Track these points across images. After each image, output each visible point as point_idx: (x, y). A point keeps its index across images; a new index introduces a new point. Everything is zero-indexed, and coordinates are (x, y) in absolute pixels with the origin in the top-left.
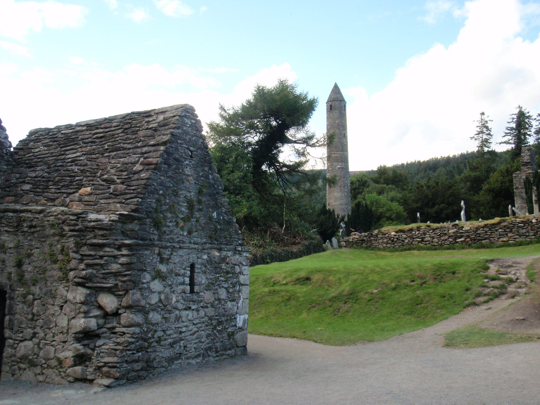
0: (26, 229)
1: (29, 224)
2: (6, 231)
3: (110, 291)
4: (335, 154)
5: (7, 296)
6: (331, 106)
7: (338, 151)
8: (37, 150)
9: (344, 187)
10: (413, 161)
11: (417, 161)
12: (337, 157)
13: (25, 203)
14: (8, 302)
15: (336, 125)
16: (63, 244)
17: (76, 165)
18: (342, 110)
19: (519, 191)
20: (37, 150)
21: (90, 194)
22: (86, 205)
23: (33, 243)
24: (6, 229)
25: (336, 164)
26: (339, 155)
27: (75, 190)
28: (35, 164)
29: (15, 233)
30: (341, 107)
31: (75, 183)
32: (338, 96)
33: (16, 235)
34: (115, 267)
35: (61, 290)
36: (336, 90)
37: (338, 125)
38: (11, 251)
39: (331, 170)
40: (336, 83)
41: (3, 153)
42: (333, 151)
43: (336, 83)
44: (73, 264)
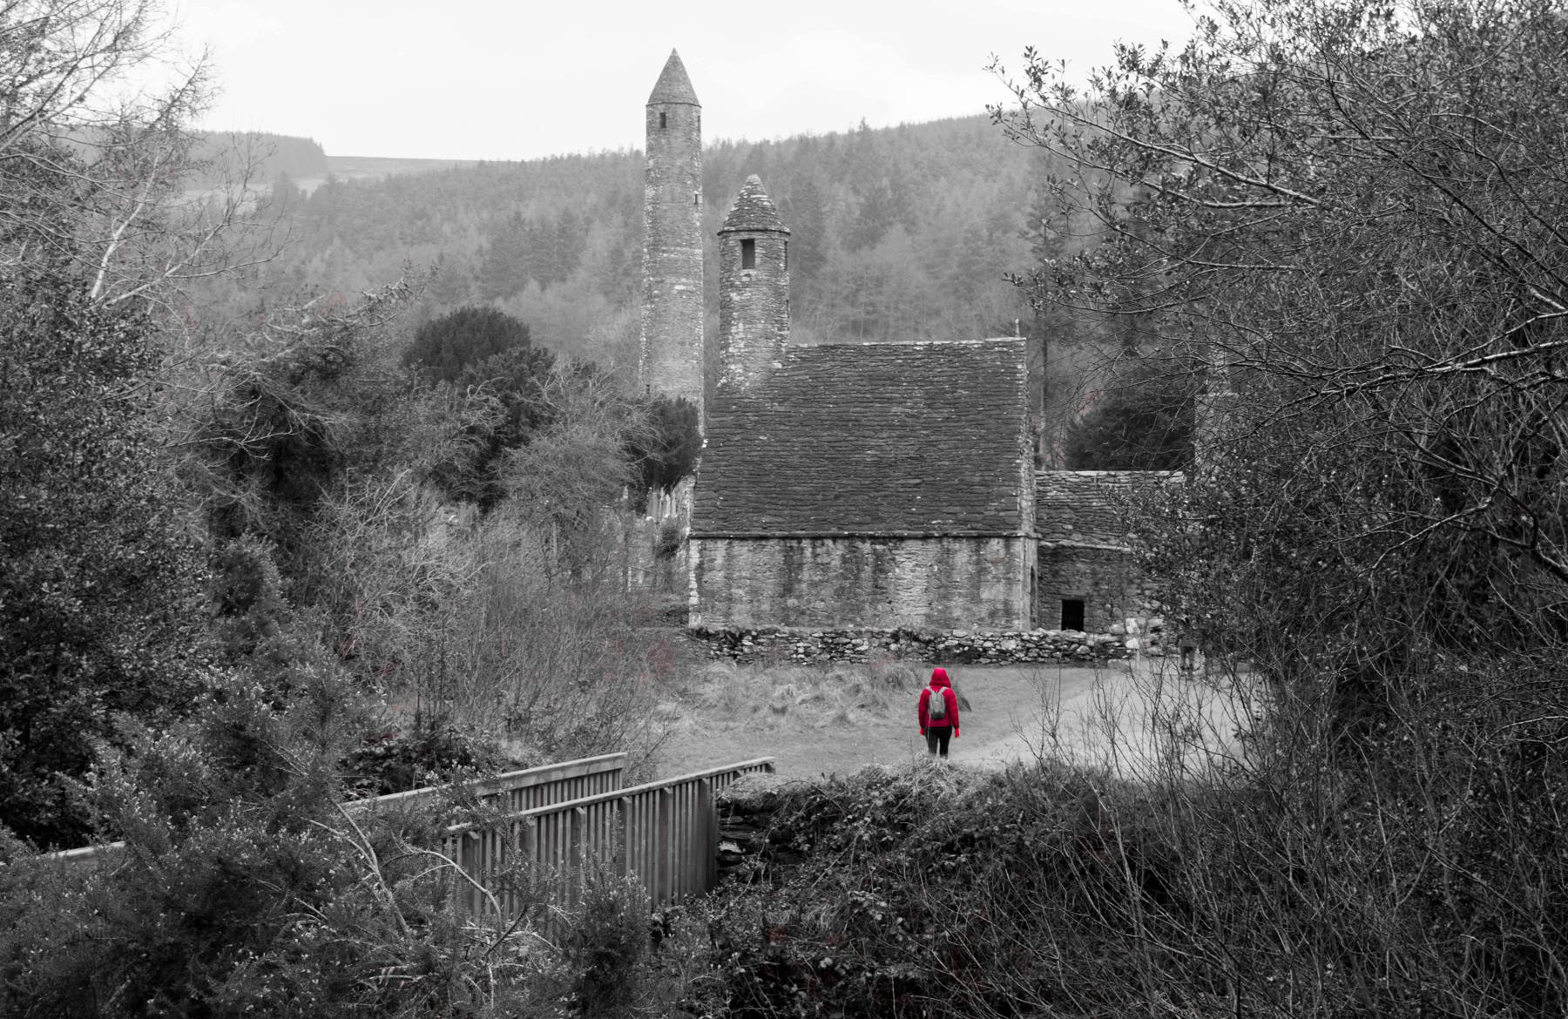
4: (672, 252)
6: (663, 115)
12: (676, 261)
14: (1086, 609)
15: (677, 171)
18: (691, 132)
25: (673, 280)
32: (682, 89)
36: (673, 70)
37: (681, 173)
39: (657, 296)
40: (674, 51)
42: (666, 244)
43: (674, 51)
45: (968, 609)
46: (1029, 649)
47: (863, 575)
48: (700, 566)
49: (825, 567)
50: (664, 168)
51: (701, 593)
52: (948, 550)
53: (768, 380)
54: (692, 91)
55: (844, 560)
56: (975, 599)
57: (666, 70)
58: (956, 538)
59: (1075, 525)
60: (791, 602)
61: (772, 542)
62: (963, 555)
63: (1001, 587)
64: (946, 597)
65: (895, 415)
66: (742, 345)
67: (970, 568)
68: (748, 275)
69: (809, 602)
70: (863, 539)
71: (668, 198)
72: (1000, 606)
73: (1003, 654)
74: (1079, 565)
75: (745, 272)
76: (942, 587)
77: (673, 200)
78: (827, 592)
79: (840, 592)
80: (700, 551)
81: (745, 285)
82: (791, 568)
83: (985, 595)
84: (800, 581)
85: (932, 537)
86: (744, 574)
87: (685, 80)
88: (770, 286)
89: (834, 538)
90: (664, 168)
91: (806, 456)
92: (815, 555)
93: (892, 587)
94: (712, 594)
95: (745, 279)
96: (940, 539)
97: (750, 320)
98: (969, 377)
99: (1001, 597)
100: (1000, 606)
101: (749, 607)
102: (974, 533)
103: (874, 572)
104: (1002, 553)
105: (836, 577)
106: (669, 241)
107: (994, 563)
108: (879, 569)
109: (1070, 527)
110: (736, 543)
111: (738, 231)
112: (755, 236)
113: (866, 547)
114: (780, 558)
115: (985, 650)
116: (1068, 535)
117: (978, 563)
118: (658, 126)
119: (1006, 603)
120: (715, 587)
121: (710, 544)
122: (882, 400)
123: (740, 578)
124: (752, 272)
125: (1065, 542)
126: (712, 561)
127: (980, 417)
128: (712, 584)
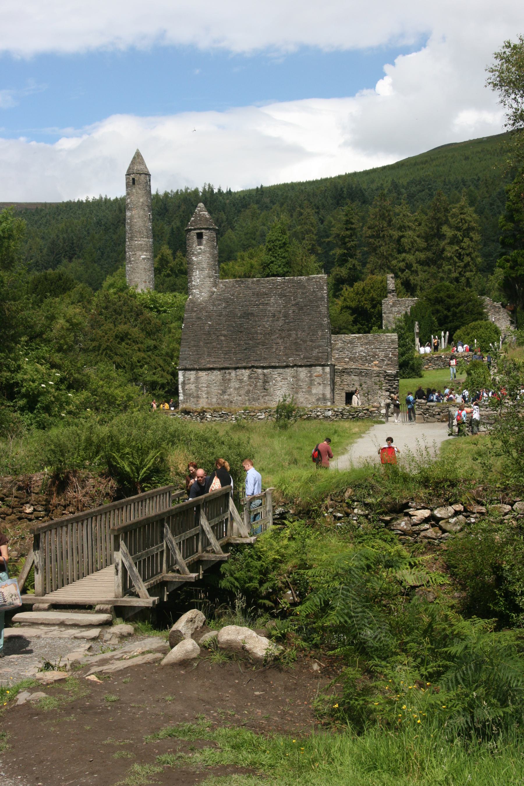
3: (393, 393)
6: (133, 179)
7: (143, 237)
9: (149, 282)
10: (97, 197)
11: (104, 197)
12: (141, 245)
15: (140, 204)
19: (387, 315)
25: (140, 253)
26: (143, 243)
30: (147, 182)
32: (142, 167)
34: (394, 386)
35: (379, 392)
36: (138, 158)
39: (133, 261)
40: (138, 150)
43: (138, 150)
44: (384, 385)
45: (306, 398)
46: (337, 415)
47: (258, 384)
48: (184, 383)
49: (241, 381)
50: (135, 203)
51: (184, 395)
53: (211, 296)
54: (146, 168)
55: (250, 377)
56: (309, 392)
57: (134, 158)
58: (301, 366)
59: (350, 358)
60: (226, 397)
62: (303, 373)
63: (321, 387)
64: (297, 393)
65: (269, 311)
66: (198, 281)
67: (307, 379)
68: (200, 249)
69: (234, 397)
70: (257, 367)
71: (137, 216)
72: (321, 396)
73: (326, 418)
75: (199, 247)
76: (296, 388)
77: (139, 217)
78: (242, 392)
79: (248, 392)
80: (184, 375)
81: (199, 253)
82: (225, 381)
83: (314, 391)
84: (230, 388)
88: (210, 254)
89: (245, 368)
90: (135, 203)
91: (230, 331)
92: (237, 376)
94: (190, 395)
95: (199, 251)
96: (293, 367)
97: (202, 270)
98: (303, 293)
99: (321, 392)
100: (321, 396)
101: (206, 400)
102: (309, 363)
103: (263, 383)
104: (321, 372)
105: (247, 385)
106: (138, 236)
107: (316, 376)
108: (265, 382)
111: (195, 229)
112: (203, 231)
113: (260, 371)
114: (220, 377)
115: (318, 416)
116: (347, 363)
117: (311, 376)
118: (131, 184)
120: (191, 392)
121: (188, 373)
122: (263, 304)
123: (203, 387)
124: (202, 247)
125: (346, 367)
126: (189, 379)
127: (308, 311)
128: (190, 390)
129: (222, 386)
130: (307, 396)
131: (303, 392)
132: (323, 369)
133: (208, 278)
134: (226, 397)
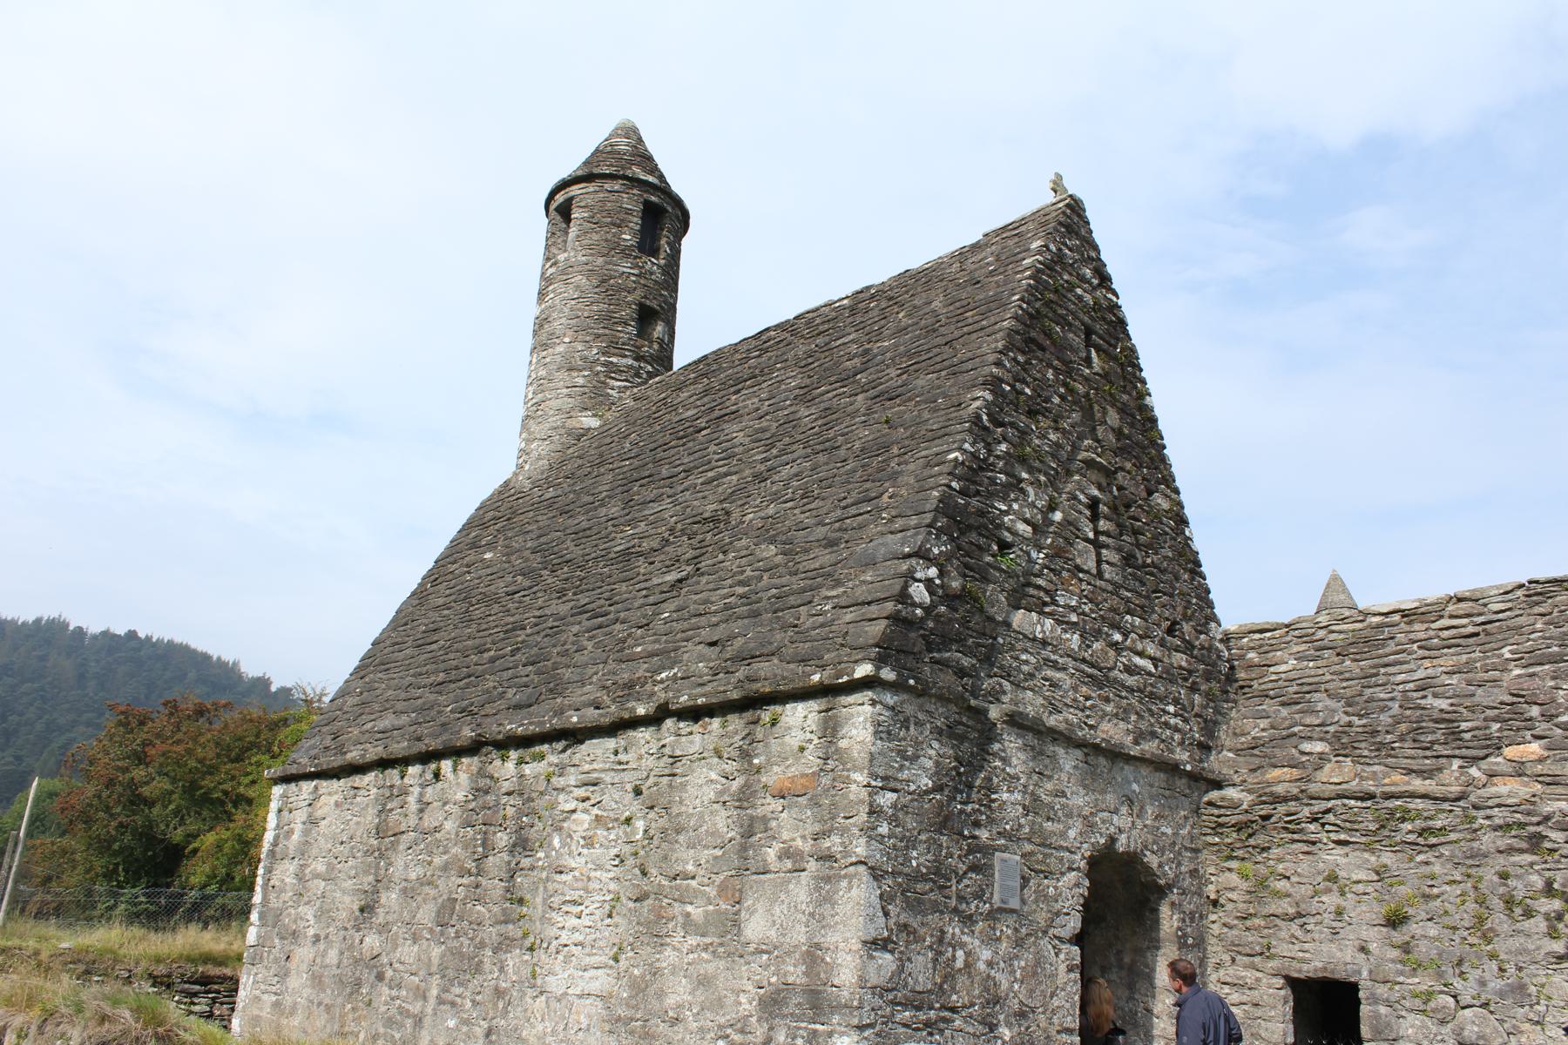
0: (1411, 838)
1: (1419, 824)
2: (1339, 843)
5: (1361, 994)
8: (1283, 668)
13: (1336, 780)
14: (1365, 1009)
16: (1548, 874)
17: (1435, 696)
20: (1283, 668)
21: (1541, 760)
22: (1549, 784)
23: (1437, 869)
24: (1343, 837)
27: (1481, 753)
28: (1301, 698)
29: (1368, 848)
31: (1467, 736)
33: (1372, 851)
38: (1360, 888)
41: (1220, 672)
45: (704, 982)
52: (676, 759)
58: (694, 714)
60: (372, 941)
61: (370, 777)
63: (800, 891)
72: (795, 973)
74: (1334, 857)
78: (426, 915)
79: (447, 914)
83: (756, 927)
85: (634, 723)
86: (320, 867)
87: (1345, 590)
89: (456, 753)
92: (424, 806)
93: (539, 900)
99: (799, 936)
100: (795, 973)
104: (812, 759)
109: (1319, 747)
110: (324, 785)
113: (506, 768)
117: (744, 798)
119: (813, 956)
123: (317, 876)
129: (367, 872)
130: (712, 966)
131: (688, 924)
132: (830, 729)
133: (563, 375)
134: (372, 941)
